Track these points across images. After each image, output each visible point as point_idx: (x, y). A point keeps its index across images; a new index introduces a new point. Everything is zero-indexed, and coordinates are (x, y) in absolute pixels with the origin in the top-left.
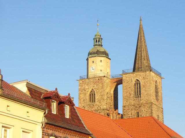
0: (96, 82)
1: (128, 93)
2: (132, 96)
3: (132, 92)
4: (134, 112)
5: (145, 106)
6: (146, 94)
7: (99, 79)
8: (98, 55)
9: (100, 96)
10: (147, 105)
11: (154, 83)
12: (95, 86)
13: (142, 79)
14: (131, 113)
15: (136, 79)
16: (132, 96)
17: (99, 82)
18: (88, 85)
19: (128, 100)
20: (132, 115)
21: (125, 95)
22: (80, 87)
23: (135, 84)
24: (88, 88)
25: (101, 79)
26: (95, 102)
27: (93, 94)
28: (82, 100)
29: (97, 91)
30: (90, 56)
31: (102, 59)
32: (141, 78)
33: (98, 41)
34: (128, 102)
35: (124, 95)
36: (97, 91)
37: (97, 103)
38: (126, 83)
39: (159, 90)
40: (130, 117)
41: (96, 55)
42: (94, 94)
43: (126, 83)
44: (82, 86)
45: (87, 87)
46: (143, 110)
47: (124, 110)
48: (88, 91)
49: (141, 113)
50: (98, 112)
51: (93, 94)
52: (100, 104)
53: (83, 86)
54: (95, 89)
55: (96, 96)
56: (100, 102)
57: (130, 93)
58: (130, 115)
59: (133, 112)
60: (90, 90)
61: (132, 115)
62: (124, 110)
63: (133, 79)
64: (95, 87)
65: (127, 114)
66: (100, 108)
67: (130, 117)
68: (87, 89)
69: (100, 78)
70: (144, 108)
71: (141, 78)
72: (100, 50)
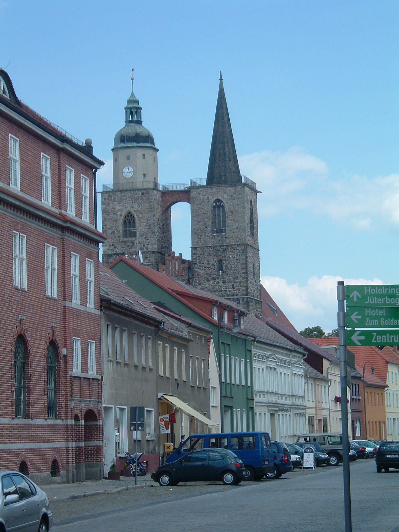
0: (137, 199)
1: (201, 224)
2: (209, 229)
4: (214, 260)
6: (235, 227)
7: (142, 194)
8: (138, 145)
9: (146, 226)
10: (238, 248)
11: (249, 204)
12: (136, 206)
13: (228, 199)
15: (215, 198)
17: (142, 199)
18: (120, 202)
19: (201, 236)
20: (209, 264)
21: (197, 227)
22: (104, 206)
23: (214, 207)
24: (121, 210)
25: (148, 193)
27: (132, 221)
29: (141, 216)
30: (123, 145)
32: (226, 196)
33: (133, 111)
39: (254, 216)
41: (135, 144)
42: (134, 222)
43: (198, 204)
44: (109, 205)
45: (118, 208)
46: (230, 256)
47: (195, 254)
51: (132, 221)
54: (135, 211)
56: (145, 238)
57: (205, 224)
58: (206, 265)
59: (211, 259)
61: (209, 264)
62: (195, 254)
66: (147, 249)
69: (144, 192)
71: (226, 196)
72: (141, 134)
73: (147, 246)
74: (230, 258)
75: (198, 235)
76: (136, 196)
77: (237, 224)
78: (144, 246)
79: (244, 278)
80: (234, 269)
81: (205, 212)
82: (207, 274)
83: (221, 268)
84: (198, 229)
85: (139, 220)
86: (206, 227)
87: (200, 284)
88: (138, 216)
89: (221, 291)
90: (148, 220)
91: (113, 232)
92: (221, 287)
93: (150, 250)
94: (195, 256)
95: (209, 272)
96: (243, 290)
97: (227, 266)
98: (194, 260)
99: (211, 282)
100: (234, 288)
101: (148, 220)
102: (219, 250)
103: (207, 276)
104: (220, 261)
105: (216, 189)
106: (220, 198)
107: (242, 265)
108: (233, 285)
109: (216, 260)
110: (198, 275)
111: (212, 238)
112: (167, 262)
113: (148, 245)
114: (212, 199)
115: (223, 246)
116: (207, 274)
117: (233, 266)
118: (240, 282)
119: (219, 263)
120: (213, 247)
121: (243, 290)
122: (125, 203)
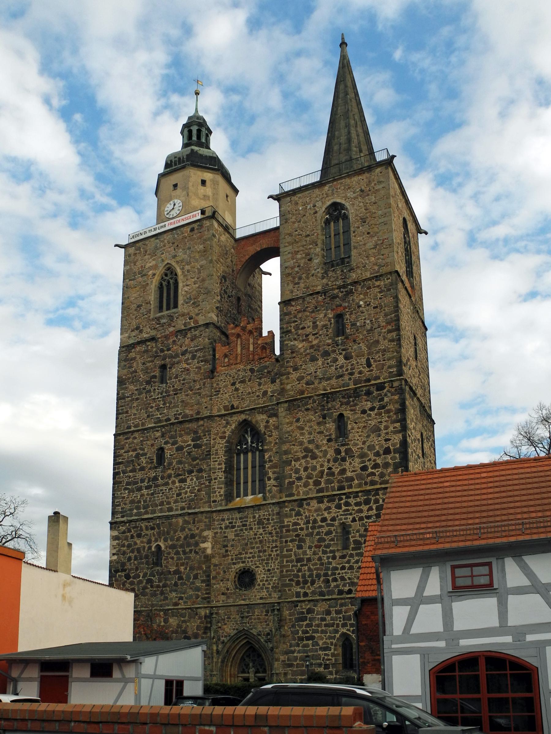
1: (299, 256)
3: (318, 250)
5: (369, 288)
6: (370, 245)
10: (377, 283)
13: (355, 198)
14: (314, 323)
15: (329, 203)
16: (316, 261)
18: (153, 254)
19: (300, 278)
20: (315, 326)
23: (327, 222)
24: (156, 267)
26: (176, 306)
28: (134, 307)
29: (187, 267)
31: (208, 176)
34: (302, 285)
35: (287, 264)
36: (187, 267)
37: (182, 307)
38: (294, 223)
40: (307, 336)
43: (294, 223)
46: (361, 303)
48: (154, 275)
49: (353, 316)
50: (189, 335)
52: (193, 311)
53: (137, 263)
54: (177, 262)
55: (180, 285)
60: (160, 271)
61: (315, 326)
63: (319, 204)
64: (178, 259)
65: (297, 328)
66: (196, 322)
67: (307, 336)
68: (150, 268)
69: (195, 226)
70: (366, 294)
73: (196, 318)
74: (360, 306)
75: (294, 278)
76: (181, 237)
77: (376, 238)
78: (191, 318)
79: (392, 341)
80: (369, 327)
81: (308, 233)
82: (312, 347)
83: (340, 330)
84: (292, 268)
85: (185, 276)
86: (310, 260)
87: (296, 369)
88: (183, 268)
89: (341, 376)
90: (199, 273)
91: (139, 306)
92: (342, 367)
93: (201, 323)
94: (287, 318)
95: (315, 342)
96: (390, 367)
97: (354, 325)
98: (285, 326)
99: (320, 362)
100: (369, 365)
101: (199, 273)
102: (337, 296)
103: (312, 350)
104: (339, 317)
105: (330, 187)
106: (338, 200)
107: (386, 315)
108: (368, 360)
109: (330, 316)
110: (292, 353)
111: (323, 278)
112: (233, 338)
113: (197, 315)
114: (322, 208)
115: (344, 286)
116: (312, 347)
117: (368, 322)
118: (384, 350)
119: (337, 322)
120: (325, 292)
121: (390, 367)
122: (163, 254)
